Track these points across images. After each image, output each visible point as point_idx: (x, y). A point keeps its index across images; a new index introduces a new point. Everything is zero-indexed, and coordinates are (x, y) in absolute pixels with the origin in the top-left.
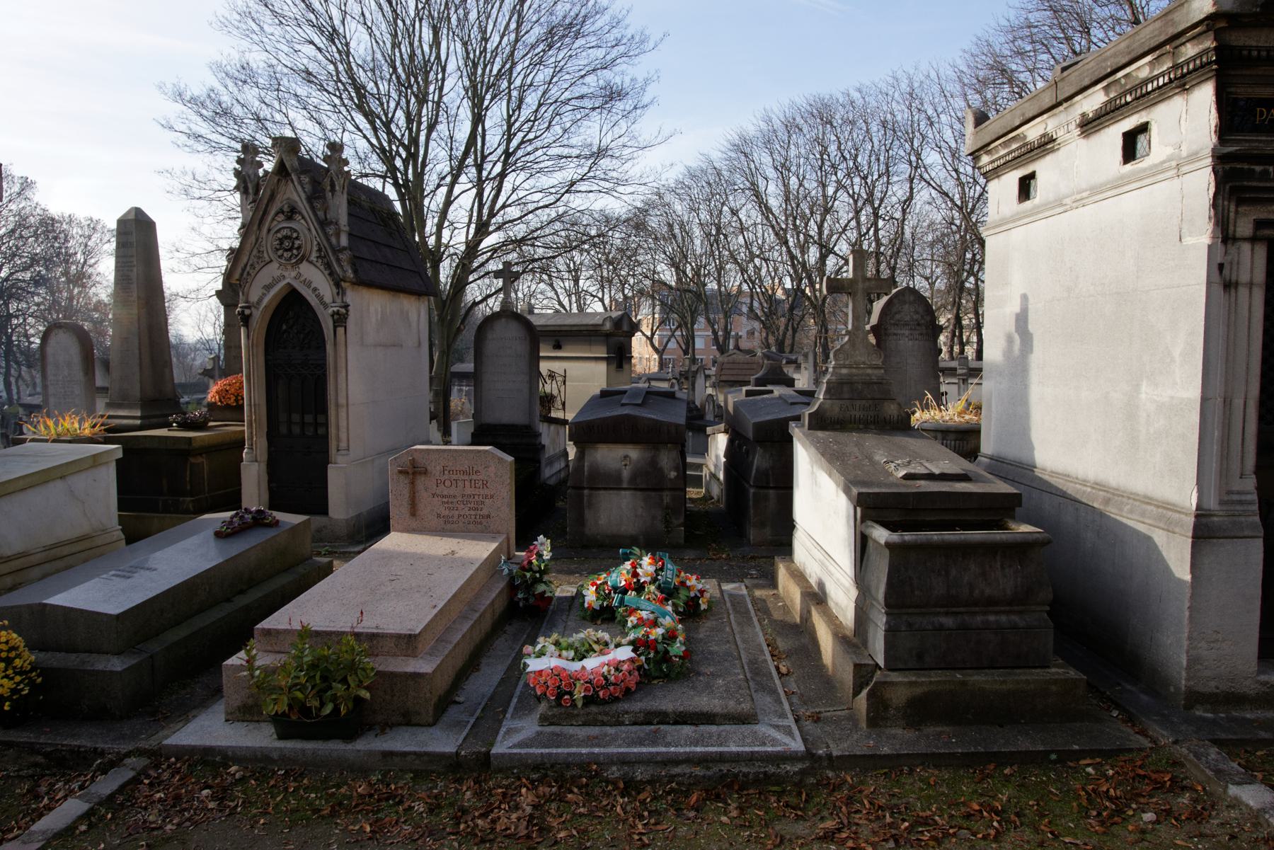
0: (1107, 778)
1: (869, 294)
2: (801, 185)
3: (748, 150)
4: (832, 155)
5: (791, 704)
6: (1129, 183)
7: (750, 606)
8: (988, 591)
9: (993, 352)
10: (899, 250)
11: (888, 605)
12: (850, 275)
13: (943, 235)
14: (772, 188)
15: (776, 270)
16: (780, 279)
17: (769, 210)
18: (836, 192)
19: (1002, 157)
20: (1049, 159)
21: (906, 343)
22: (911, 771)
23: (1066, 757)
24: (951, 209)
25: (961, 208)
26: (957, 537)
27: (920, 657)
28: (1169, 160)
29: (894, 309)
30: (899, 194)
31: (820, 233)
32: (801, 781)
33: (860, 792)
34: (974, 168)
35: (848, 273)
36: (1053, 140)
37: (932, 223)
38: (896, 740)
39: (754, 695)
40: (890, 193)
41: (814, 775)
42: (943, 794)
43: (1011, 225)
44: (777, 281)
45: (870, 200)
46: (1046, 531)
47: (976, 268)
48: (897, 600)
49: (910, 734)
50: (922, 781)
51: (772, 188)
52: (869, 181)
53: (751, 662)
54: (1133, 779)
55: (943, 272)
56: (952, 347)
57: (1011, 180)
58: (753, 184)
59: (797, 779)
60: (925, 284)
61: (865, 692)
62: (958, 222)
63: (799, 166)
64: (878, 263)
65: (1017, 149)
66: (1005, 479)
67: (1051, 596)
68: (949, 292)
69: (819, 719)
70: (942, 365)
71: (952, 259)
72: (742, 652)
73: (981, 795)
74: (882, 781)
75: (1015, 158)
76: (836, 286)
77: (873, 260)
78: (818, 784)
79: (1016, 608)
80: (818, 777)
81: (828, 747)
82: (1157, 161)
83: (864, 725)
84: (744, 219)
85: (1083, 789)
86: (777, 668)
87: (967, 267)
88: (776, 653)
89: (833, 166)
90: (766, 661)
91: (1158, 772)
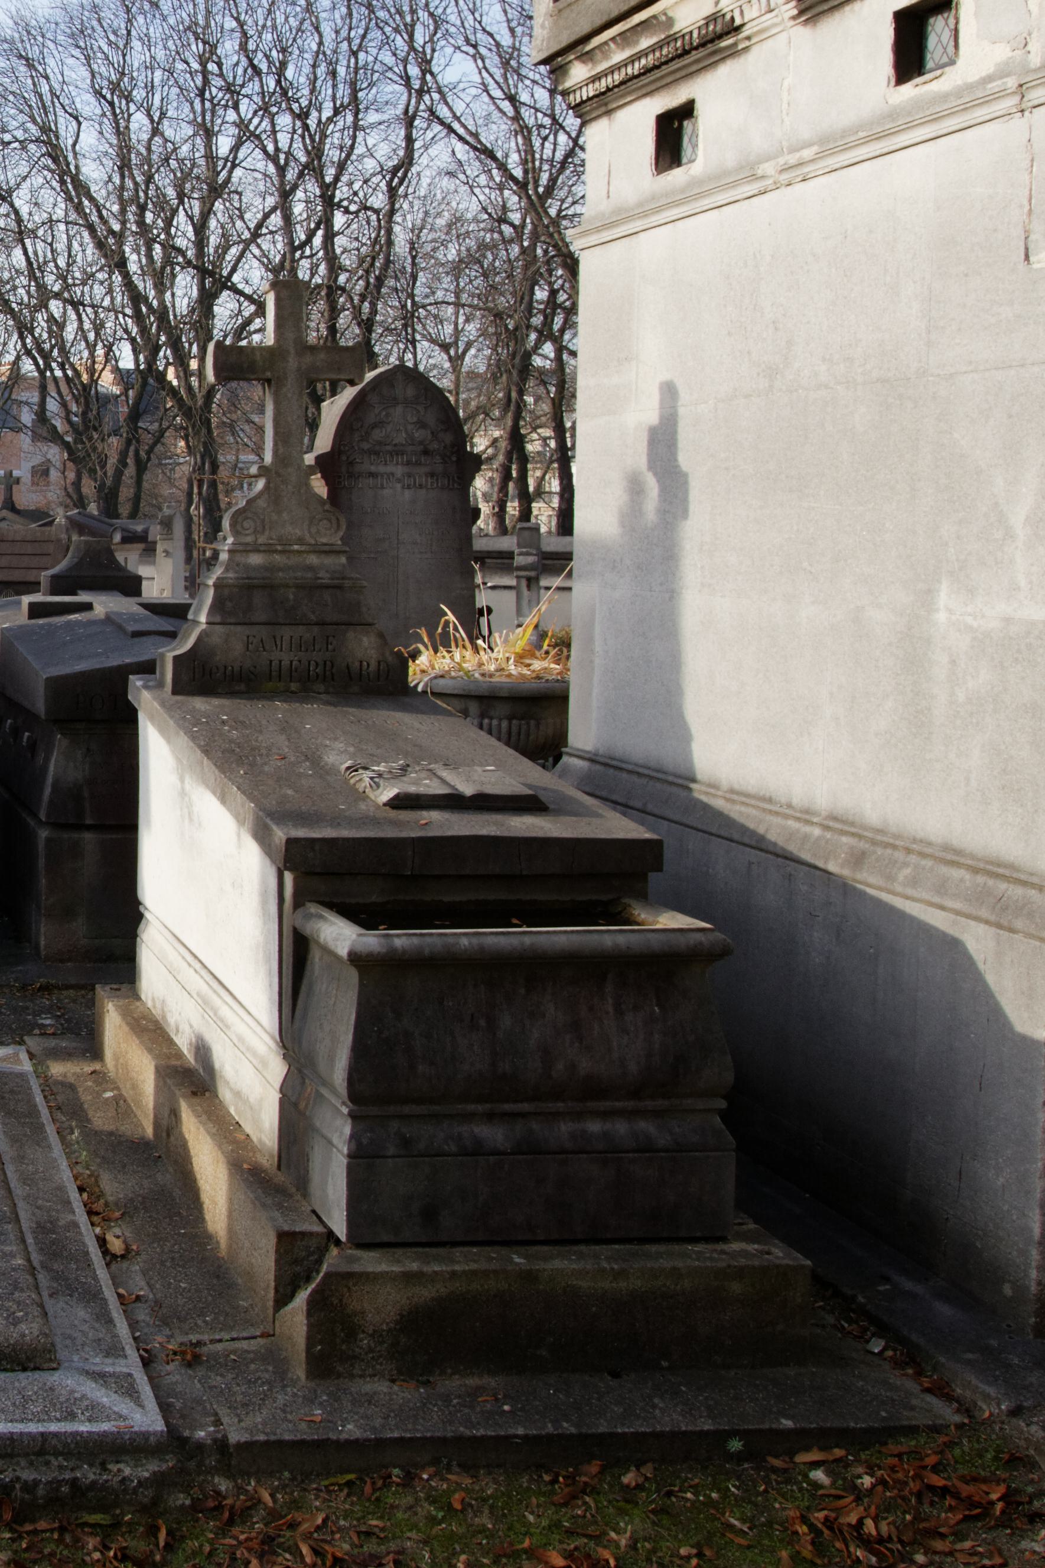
0: (860, 1497)
1: (312, 383)
2: (156, 132)
3: (34, 53)
4: (227, 64)
5: (133, 1325)
6: (909, 127)
7: (39, 1099)
8: (585, 1065)
9: (597, 515)
10: (380, 281)
11: (355, 1096)
12: (269, 338)
13: (482, 246)
14: (89, 139)
15: (98, 327)
16: (109, 349)
17: (82, 188)
18: (235, 149)
19: (618, 67)
20: (725, 71)
21: (398, 496)
22: (409, 1479)
23: (765, 1447)
24: (501, 188)
25: (522, 186)
26: (514, 941)
27: (429, 1215)
28: (1002, 73)
29: (371, 418)
30: (383, 151)
31: (200, 242)
32: (155, 1502)
33: (293, 1526)
34: (552, 92)
35: (265, 334)
36: (734, 29)
37: (457, 220)
38: (376, 1406)
39: (49, 1303)
40: (359, 150)
41: (186, 1489)
42: (483, 1530)
43: (638, 225)
44: (100, 351)
45: (314, 166)
46: (718, 928)
47: (558, 321)
48: (382, 1083)
49: (405, 1394)
50: (433, 1501)
51: (89, 139)
52: (312, 122)
53: (42, 1229)
54: (919, 1495)
55: (483, 333)
56: (502, 505)
57: (640, 117)
58: (45, 129)
59: (146, 1495)
60: (441, 359)
61: (302, 1297)
62: (515, 217)
63: (150, 88)
64: (334, 311)
65: (652, 49)
66: (624, 807)
67: (729, 1077)
68: (495, 378)
69: (197, 1357)
70: (479, 545)
71: (503, 302)
72: (21, 1205)
73: (570, 1533)
74: (342, 1501)
75: (647, 71)
76: (237, 364)
77: (322, 304)
78: (196, 1507)
79: (649, 1104)
80: (196, 1492)
81: (218, 1422)
82: (973, 76)
83: (300, 1372)
84: (24, 211)
85: (804, 1520)
86: (102, 1242)
87: (537, 320)
88: (98, 1206)
89: (230, 88)
90: (75, 1225)
91: (975, 1479)
